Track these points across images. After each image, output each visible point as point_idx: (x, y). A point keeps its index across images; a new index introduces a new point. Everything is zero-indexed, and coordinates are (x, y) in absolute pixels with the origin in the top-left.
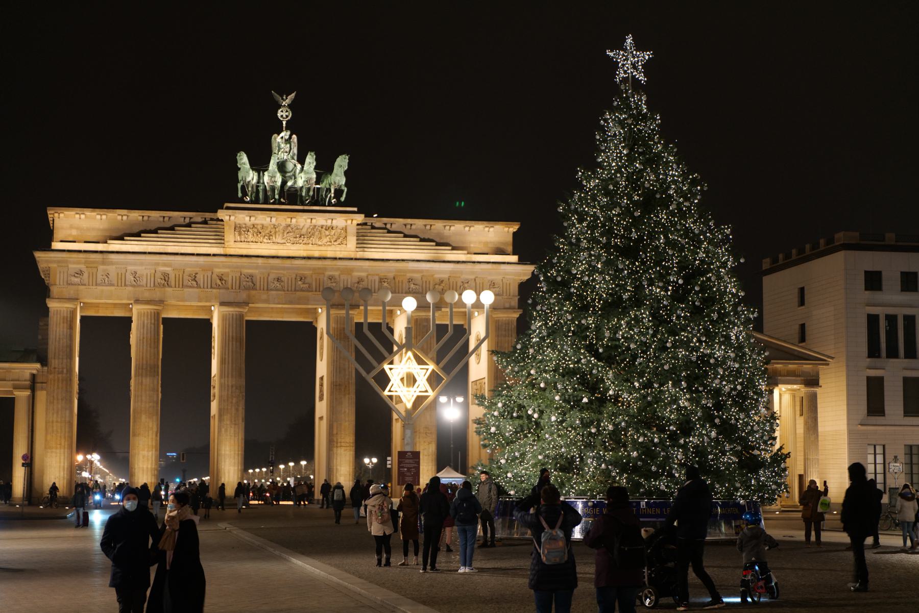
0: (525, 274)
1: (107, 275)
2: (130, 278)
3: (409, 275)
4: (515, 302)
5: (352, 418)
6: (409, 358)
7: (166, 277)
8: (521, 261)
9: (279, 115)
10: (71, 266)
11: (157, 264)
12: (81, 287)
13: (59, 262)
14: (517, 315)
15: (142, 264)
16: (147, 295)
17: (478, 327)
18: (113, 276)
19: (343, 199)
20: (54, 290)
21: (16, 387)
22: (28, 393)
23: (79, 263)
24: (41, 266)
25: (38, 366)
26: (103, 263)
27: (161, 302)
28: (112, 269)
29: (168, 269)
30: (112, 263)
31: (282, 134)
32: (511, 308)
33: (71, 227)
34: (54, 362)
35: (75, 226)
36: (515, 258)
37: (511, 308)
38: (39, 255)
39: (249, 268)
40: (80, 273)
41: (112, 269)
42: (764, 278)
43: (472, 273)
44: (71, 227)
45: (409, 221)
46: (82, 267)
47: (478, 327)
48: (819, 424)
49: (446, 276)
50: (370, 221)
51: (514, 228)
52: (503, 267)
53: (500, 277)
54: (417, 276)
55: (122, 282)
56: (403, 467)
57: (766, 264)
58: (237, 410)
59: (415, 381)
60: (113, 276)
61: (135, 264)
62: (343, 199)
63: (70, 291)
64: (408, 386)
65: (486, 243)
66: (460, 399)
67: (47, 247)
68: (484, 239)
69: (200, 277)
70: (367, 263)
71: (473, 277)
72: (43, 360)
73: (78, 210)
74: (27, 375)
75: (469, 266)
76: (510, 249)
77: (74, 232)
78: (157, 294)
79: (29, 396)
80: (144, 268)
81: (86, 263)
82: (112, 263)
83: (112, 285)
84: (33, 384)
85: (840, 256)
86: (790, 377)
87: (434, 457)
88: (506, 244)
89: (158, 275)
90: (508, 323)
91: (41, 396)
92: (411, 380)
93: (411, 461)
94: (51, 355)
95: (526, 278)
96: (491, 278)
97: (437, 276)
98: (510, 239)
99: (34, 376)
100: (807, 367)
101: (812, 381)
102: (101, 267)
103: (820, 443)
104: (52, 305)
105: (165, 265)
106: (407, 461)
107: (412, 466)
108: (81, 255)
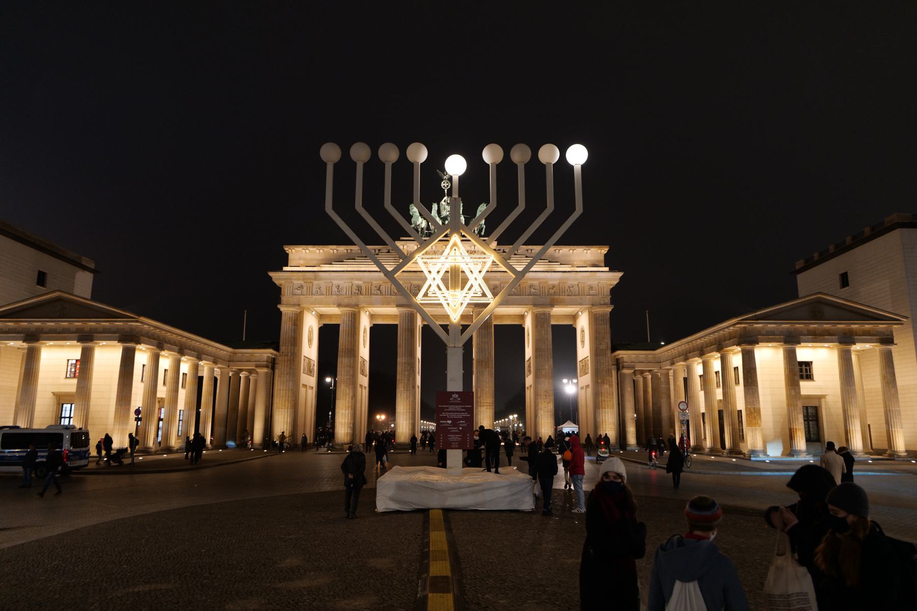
0: (614, 280)
1: (320, 288)
2: (335, 289)
3: (530, 282)
4: (608, 300)
5: (493, 385)
6: (455, 244)
7: (359, 288)
8: (611, 270)
9: (442, 185)
10: (295, 282)
11: (353, 279)
12: (302, 297)
13: (285, 279)
14: (609, 309)
15: (342, 279)
16: (346, 301)
17: (583, 324)
18: (323, 289)
19: (483, 233)
20: (284, 299)
21: (257, 366)
22: (265, 370)
23: (299, 279)
24: (277, 282)
25: (271, 351)
26: (315, 279)
27: (357, 305)
28: (322, 283)
29: (360, 283)
30: (321, 279)
31: (445, 198)
32: (605, 304)
33: (300, 259)
34: (282, 348)
35: (302, 257)
36: (607, 269)
37: (605, 304)
38: (275, 276)
39: (416, 280)
40: (302, 287)
41: (322, 283)
42: (798, 276)
43: (576, 279)
44: (300, 259)
45: (530, 247)
46: (301, 282)
47: (583, 324)
48: (897, 379)
49: (556, 282)
50: (502, 248)
51: (605, 250)
52: (598, 274)
53: (596, 282)
54: (536, 283)
55: (329, 292)
56: (445, 418)
57: (800, 264)
58: (408, 380)
59: (465, 280)
60: (323, 289)
61: (337, 279)
62: (483, 233)
63: (295, 299)
64: (455, 287)
65: (585, 261)
66: (575, 381)
67: (281, 270)
68: (583, 258)
69: (383, 288)
70: (499, 274)
71: (576, 283)
72: (277, 349)
73: (304, 247)
74: (265, 359)
75: (573, 274)
76: (603, 264)
77: (302, 262)
78: (353, 300)
79: (266, 373)
80: (342, 282)
81: (303, 279)
82: (321, 279)
83: (322, 294)
84: (272, 364)
85: (896, 234)
86: (867, 336)
87: (552, 413)
88: (600, 261)
89: (354, 287)
90: (603, 315)
91: (277, 371)
92: (455, 279)
93: (458, 408)
94: (281, 343)
95: (616, 282)
96: (589, 283)
97: (550, 283)
98: (602, 258)
99: (274, 359)
100: (882, 327)
101: (887, 340)
102: (315, 282)
103: (900, 396)
104: (283, 309)
105: (358, 279)
106: (451, 408)
107: (459, 416)
108: (300, 274)
